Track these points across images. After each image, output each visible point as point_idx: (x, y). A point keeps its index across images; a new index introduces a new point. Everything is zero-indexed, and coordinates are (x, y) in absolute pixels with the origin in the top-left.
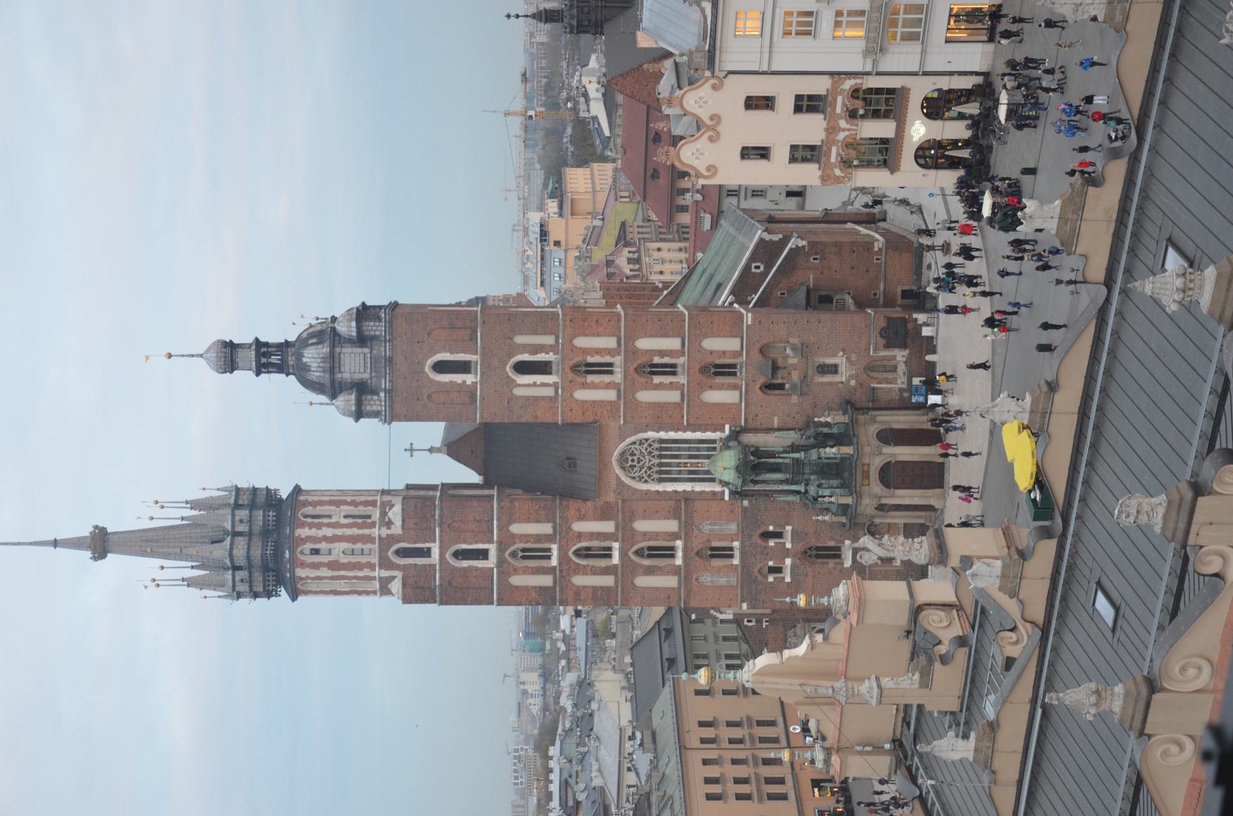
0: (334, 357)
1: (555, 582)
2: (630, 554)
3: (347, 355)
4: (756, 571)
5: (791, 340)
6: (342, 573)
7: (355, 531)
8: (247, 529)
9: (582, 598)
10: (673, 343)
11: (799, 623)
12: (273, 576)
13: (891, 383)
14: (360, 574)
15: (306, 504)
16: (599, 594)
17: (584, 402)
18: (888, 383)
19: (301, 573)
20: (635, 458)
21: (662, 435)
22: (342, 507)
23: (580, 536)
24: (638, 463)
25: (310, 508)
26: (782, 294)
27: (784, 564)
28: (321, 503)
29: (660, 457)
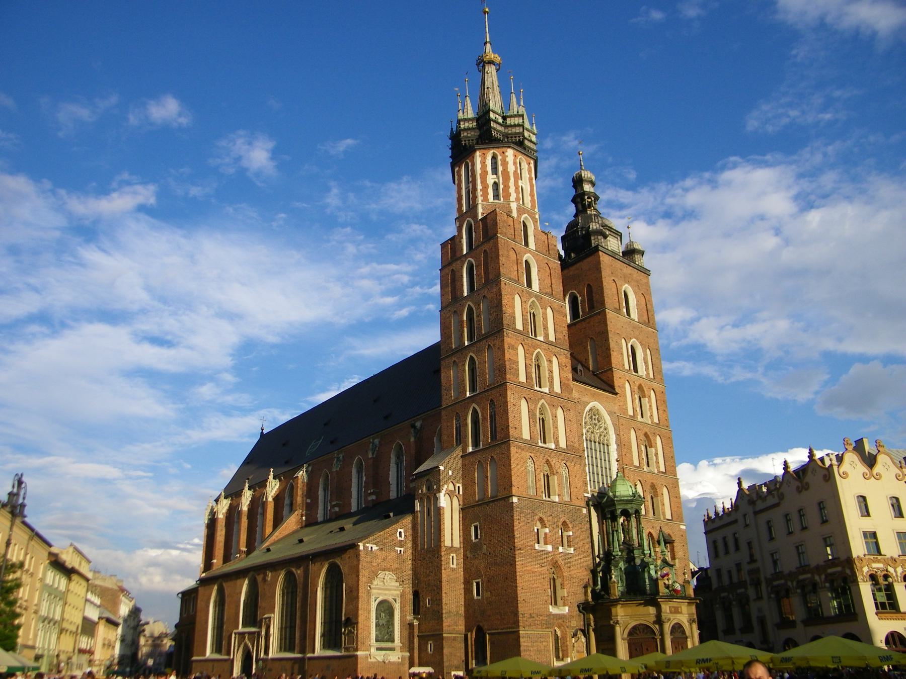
0: (616, 234)
1: (519, 332)
2: (543, 400)
3: (617, 243)
4: (541, 515)
5: (677, 561)
6: (512, 179)
9: (510, 350)
11: (400, 585)
12: (500, 138)
14: (512, 190)
17: (625, 389)
19: (510, 153)
20: (597, 422)
23: (550, 361)
27: (546, 543)
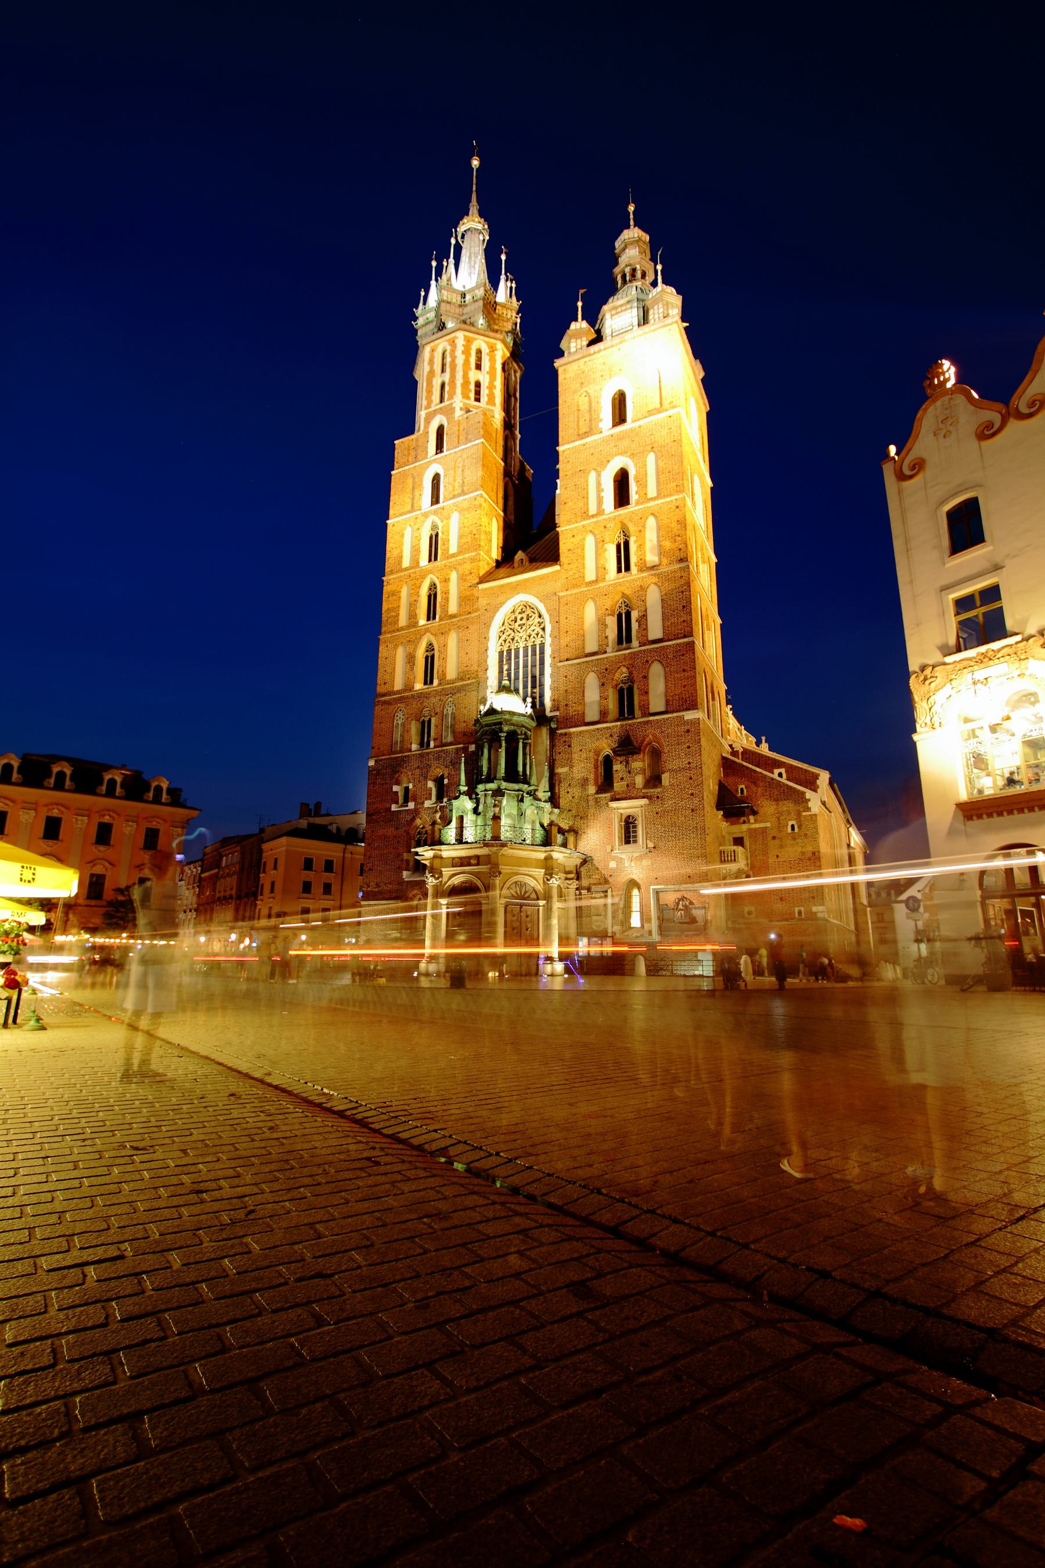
1: (406, 569)
7: (459, 381)
8: (467, 302)
10: (655, 631)
13: (614, 917)
15: (492, 349)
16: (393, 614)
18: (613, 913)
21: (548, 641)
22: (487, 377)
23: (446, 581)
24: (521, 626)
25: (487, 351)
26: (742, 790)
28: (492, 360)
29: (526, 648)
